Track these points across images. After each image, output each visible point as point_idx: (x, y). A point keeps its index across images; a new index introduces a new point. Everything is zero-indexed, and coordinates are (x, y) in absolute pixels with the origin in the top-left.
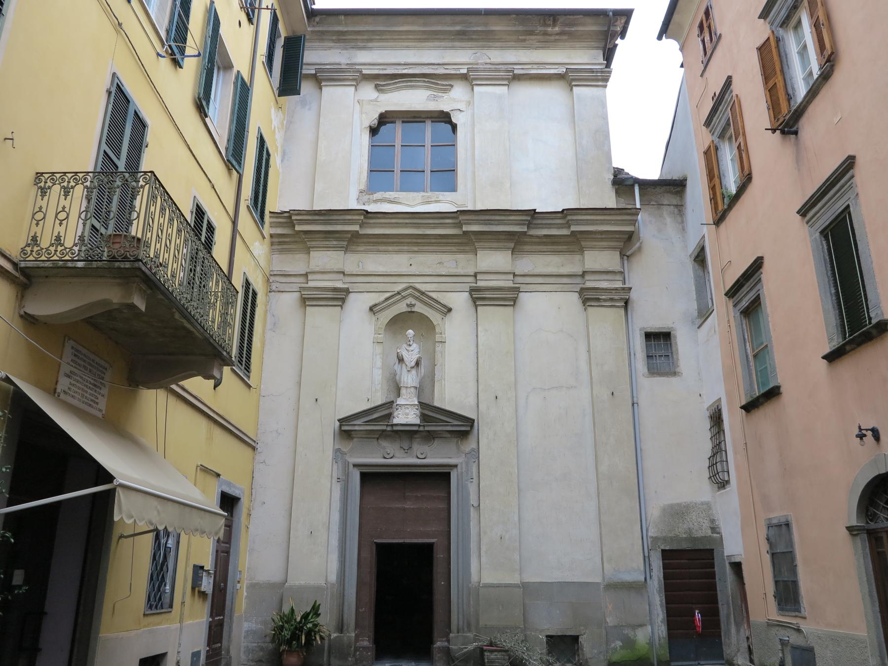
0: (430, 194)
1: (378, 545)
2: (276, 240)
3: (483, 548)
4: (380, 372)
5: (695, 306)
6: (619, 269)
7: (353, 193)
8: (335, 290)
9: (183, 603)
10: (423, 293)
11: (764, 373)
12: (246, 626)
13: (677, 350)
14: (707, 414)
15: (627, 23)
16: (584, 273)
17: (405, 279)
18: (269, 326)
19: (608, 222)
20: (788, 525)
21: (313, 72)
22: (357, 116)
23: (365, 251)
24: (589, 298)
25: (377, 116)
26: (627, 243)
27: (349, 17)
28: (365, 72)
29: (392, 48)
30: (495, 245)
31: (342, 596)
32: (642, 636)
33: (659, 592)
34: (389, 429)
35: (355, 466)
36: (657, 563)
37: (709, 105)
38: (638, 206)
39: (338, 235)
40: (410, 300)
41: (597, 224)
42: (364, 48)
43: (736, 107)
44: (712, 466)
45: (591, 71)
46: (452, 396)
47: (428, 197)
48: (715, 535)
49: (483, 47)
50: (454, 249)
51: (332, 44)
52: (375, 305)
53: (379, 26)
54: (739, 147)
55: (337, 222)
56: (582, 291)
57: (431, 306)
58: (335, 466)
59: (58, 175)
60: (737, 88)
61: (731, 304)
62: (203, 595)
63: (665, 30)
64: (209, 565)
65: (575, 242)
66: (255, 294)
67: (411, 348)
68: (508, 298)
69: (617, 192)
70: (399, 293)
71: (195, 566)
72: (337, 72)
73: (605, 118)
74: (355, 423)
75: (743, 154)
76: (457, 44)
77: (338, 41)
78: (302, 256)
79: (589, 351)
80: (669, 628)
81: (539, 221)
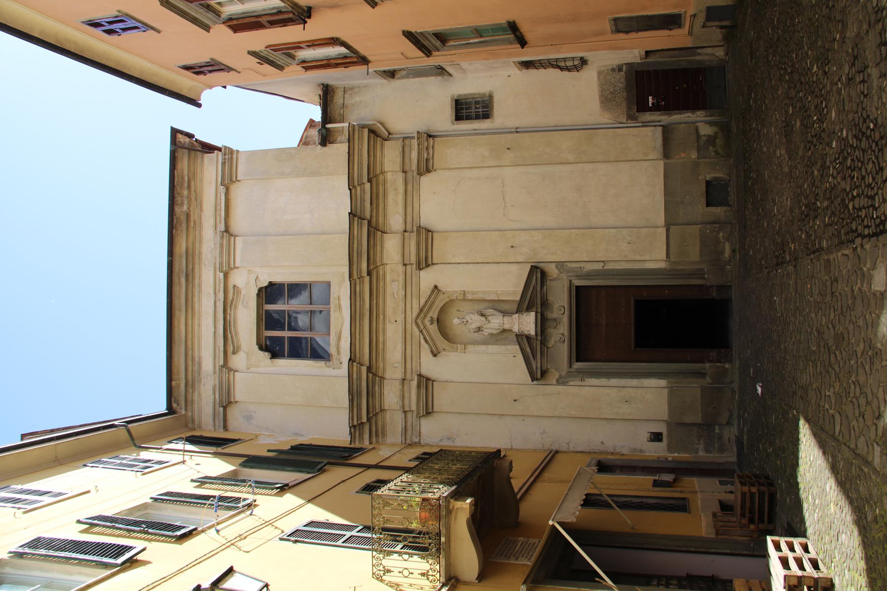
0: (332, 305)
1: (637, 345)
2: (374, 440)
3: (638, 258)
4: (490, 347)
5: (432, 79)
6: (400, 142)
7: (330, 371)
8: (419, 386)
10: (421, 311)
11: (496, 29)
12: (701, 453)
13: (470, 94)
14: (525, 71)
15: (181, 132)
16: (404, 172)
17: (409, 326)
20: (615, 20)
21: (221, 409)
22: (261, 370)
23: (384, 361)
24: (425, 167)
25: (261, 352)
26: (376, 134)
27: (174, 377)
28: (222, 363)
29: (199, 340)
31: (677, 374)
32: (706, 130)
33: (670, 115)
34: (539, 338)
35: (570, 367)
36: (648, 117)
37: (267, 68)
38: (346, 125)
39: (370, 385)
40: (427, 322)
43: (275, 48)
44: (568, 69)
45: (224, 164)
46: (510, 283)
48: (624, 69)
49: (200, 258)
50: (381, 284)
52: (432, 352)
54: (308, 46)
55: (359, 386)
56: (420, 174)
58: (571, 383)
60: (259, 47)
61: (435, 53)
64: (651, 478)
65: (374, 177)
66: (425, 454)
67: (470, 321)
68: (425, 235)
70: (421, 331)
72: (222, 388)
73: (264, 153)
74: (534, 367)
75: (314, 44)
76: (197, 281)
77: (193, 386)
78: (388, 415)
79: (472, 168)
80: (699, 109)
81: (359, 209)
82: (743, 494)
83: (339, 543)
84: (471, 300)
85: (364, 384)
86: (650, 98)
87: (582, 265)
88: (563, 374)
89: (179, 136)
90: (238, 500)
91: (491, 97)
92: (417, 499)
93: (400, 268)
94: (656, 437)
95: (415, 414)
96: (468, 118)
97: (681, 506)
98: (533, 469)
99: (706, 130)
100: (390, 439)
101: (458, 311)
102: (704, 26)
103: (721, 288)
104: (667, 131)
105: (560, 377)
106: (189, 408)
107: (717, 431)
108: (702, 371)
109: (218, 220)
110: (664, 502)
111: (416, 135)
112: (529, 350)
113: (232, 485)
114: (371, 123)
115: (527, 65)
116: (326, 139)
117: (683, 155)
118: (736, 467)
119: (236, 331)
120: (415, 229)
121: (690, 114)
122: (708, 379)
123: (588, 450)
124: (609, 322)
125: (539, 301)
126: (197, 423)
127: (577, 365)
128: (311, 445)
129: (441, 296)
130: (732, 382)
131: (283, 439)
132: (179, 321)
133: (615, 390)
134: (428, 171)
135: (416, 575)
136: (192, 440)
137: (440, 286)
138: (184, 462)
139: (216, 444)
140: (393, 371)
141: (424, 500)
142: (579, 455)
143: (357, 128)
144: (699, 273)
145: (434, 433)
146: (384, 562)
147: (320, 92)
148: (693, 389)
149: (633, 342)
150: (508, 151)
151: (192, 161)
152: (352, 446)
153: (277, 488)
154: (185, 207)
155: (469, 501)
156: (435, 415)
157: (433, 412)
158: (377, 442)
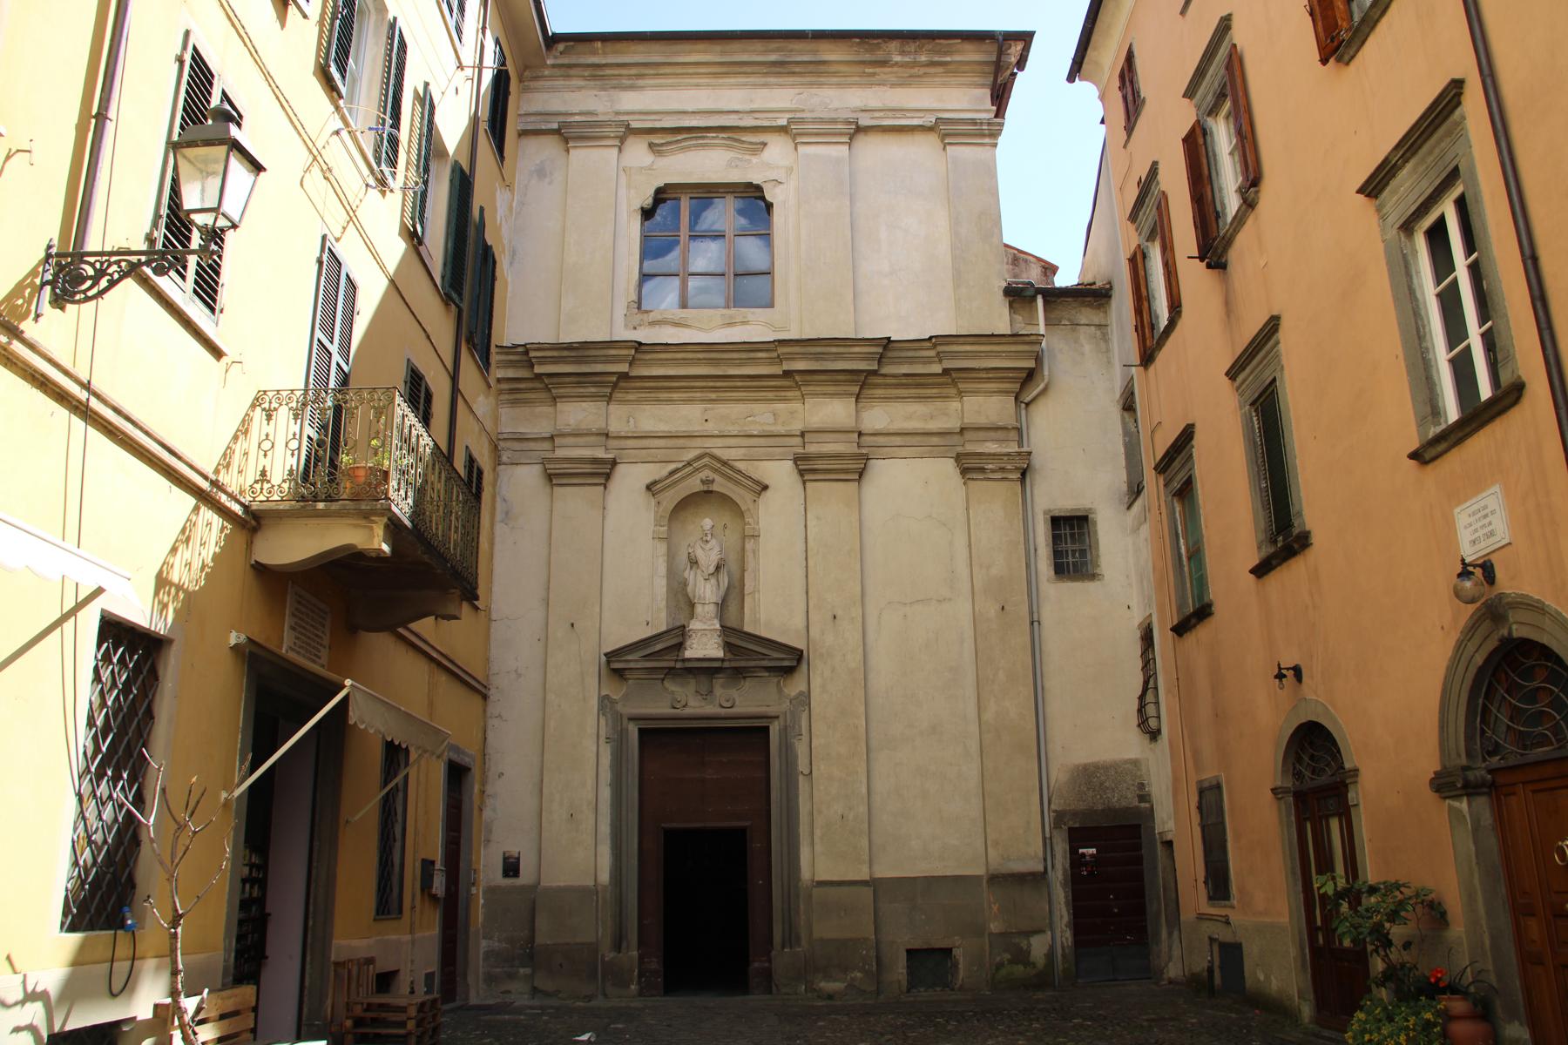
0: (733, 311)
2: (505, 386)
3: (818, 833)
4: (664, 582)
6: (1012, 422)
7: (620, 310)
8: (595, 461)
9: (413, 908)
10: (725, 463)
11: (1201, 583)
14: (1138, 634)
15: (1027, 49)
16: (962, 430)
17: (698, 442)
18: (499, 516)
19: (997, 355)
21: (555, 126)
22: (622, 192)
23: (639, 401)
24: (970, 467)
25: (652, 192)
26: (1026, 382)
27: (609, 46)
28: (634, 125)
29: (672, 86)
30: (831, 389)
31: (620, 901)
32: (1038, 947)
33: (1064, 885)
34: (679, 665)
35: (630, 719)
36: (1061, 847)
37: (1133, 193)
40: (706, 474)
41: (980, 358)
42: (632, 88)
44: (1141, 709)
45: (973, 122)
46: (773, 614)
47: (731, 317)
49: (811, 84)
50: (770, 395)
51: (582, 83)
52: (655, 483)
53: (655, 53)
56: (958, 458)
57: (737, 483)
58: (603, 722)
59: (285, 394)
61: (1161, 482)
62: (434, 897)
63: (1077, 69)
64: (438, 856)
65: (952, 380)
66: (480, 473)
68: (855, 469)
69: (1011, 306)
70: (689, 464)
71: (424, 861)
73: (994, 192)
76: (772, 80)
77: (594, 77)
81: (896, 354)
82: (403, 1009)
83: (319, 334)
84: (743, 549)
85: (599, 368)
86: (1093, 851)
87: (805, 738)
88: (619, 707)
89: (1020, 46)
90: (393, 163)
91: (1093, 577)
92: (386, 463)
93: (797, 427)
94: (511, 867)
95: (549, 455)
96: (1056, 539)
97: (387, 905)
98: (452, 657)
99: (1038, 947)
100: (506, 413)
101: (725, 527)
102: (1212, 940)
103: (768, 975)
104: (1037, 879)
105: (613, 702)
106: (557, 72)
107: (522, 971)
108: (624, 945)
109: (877, 114)
110: (395, 879)
111: (1025, 449)
112: (659, 647)
113: (419, 150)
114: (1046, 373)
115: (1147, 638)
116: (1018, 296)
117: (995, 908)
118: (458, 1003)
119: (688, 148)
120: (864, 451)
121: (1066, 919)
122: (610, 956)
123: (489, 750)
124: (709, 785)
125: (743, 664)
126: (532, 84)
127: (633, 730)
128: (494, 279)
129: (749, 496)
130: (605, 995)
131: (505, 231)
132: (705, 52)
133: (591, 796)
134: (964, 472)
135: (263, 462)
136: (501, 80)
137: (768, 493)
138: (461, 67)
139: (496, 117)
140: (623, 416)
141: (386, 474)
142: (480, 735)
143: (1036, 348)
144: (791, 939)
145: (517, 488)
146: (284, 410)
147: (1099, 284)
148: (592, 929)
149: (674, 825)
150: (998, 607)
151: (978, 68)
152: (493, 349)
153: (414, 226)
154: (898, 58)
155: (385, 548)
156: (548, 489)
157: (552, 486)
158: (500, 392)
